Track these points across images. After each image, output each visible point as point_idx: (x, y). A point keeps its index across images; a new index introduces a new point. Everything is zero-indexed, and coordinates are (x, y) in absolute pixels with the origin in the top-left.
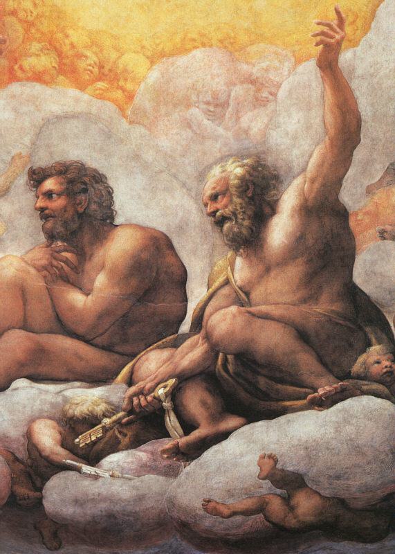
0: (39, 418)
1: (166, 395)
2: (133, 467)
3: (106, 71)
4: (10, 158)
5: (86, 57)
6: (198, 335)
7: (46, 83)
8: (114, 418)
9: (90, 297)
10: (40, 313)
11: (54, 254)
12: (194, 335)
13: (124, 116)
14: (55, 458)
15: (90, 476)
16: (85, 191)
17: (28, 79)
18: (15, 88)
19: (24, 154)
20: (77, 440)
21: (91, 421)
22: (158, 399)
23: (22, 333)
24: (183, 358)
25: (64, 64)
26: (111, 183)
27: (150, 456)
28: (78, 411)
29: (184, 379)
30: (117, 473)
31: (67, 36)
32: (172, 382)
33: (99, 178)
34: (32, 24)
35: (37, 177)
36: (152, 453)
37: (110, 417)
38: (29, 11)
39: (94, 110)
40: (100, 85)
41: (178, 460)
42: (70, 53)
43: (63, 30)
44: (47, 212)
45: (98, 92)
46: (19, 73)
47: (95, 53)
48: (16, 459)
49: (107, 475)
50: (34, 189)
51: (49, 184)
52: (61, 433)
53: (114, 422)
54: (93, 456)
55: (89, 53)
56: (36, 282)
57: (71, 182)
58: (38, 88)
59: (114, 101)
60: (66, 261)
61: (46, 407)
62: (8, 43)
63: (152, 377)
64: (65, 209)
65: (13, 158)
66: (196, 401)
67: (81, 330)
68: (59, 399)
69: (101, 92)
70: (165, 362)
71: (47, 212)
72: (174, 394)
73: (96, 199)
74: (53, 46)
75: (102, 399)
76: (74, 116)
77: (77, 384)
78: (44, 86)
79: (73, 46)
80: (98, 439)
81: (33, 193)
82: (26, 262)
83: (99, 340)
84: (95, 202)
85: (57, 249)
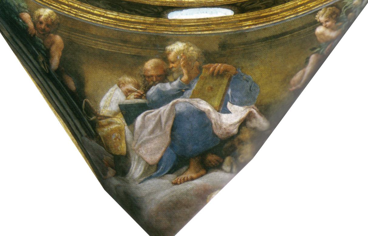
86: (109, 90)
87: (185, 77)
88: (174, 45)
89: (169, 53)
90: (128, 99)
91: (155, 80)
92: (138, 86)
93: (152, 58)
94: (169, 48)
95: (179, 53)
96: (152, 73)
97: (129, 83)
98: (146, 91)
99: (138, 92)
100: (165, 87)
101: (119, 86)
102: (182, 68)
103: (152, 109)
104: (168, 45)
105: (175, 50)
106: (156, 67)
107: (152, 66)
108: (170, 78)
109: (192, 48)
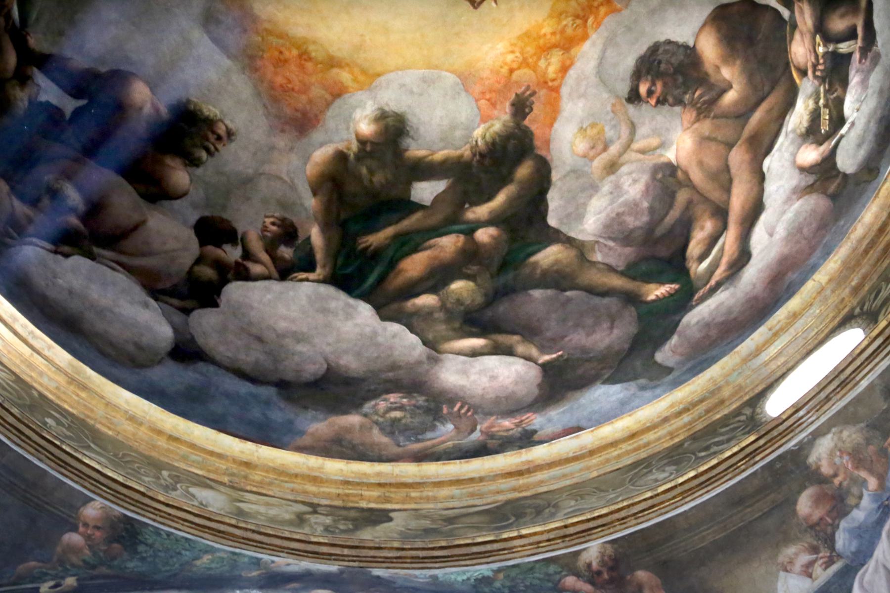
0: (795, 157)
1: (825, 46)
2: (859, 91)
3: (581, 14)
4: (612, 115)
5: (566, 25)
6: (796, 5)
7: (572, 64)
8: (822, 95)
9: (734, 86)
10: (726, 131)
11: (693, 104)
12: (794, 8)
13: (619, 11)
14: (826, 153)
15: (849, 129)
16: (660, 62)
17: (563, 77)
18: (565, 91)
19: (613, 101)
20: (823, 131)
21: (815, 116)
22: (825, 54)
23: (735, 148)
24: (805, 23)
25: (564, 45)
26: (662, 39)
27: (858, 74)
28: (805, 124)
29: (821, 29)
30: (857, 106)
31: (545, 35)
32: (818, 38)
33: (655, 48)
34: (525, 59)
35: (634, 97)
36: (857, 71)
37: (819, 99)
38: (516, 59)
39: (606, 34)
40: (590, 21)
41: (870, 51)
42: (558, 37)
43: (539, 37)
44: (661, 99)
45: (594, 26)
46: (556, 83)
47: (567, 17)
48: (812, 185)
49: (855, 114)
50: (641, 103)
51: (643, 89)
52: (812, 143)
53: (825, 96)
54: (839, 120)
55: (564, 23)
56: (706, 127)
57: (648, 72)
58: (572, 73)
59: (606, 14)
60: (701, 96)
61: (791, 149)
62: (531, 84)
63: (808, 55)
64: (665, 85)
65: (613, 112)
66: (838, 24)
67: (753, 100)
68: (791, 136)
69: (595, 23)
70: (803, 40)
71: (661, 99)
72: (828, 39)
73: (669, 55)
74: (546, 50)
75: (805, 101)
76: (604, 51)
77: (788, 117)
78: (573, 67)
79: (554, 33)
80: (830, 114)
81: (644, 105)
82: (688, 128)
83: (766, 88)
84: (671, 57)
85: (690, 100)
86: (777, 589)
87: (873, 483)
88: (814, 450)
89: (818, 468)
90: (816, 579)
91: (829, 520)
92: (815, 550)
93: (799, 492)
94: (812, 459)
95: (831, 454)
96: (817, 514)
97: (796, 554)
98: (832, 548)
99: (822, 558)
100: (853, 519)
101: (787, 571)
102: (856, 472)
103: (863, 565)
104: (807, 457)
105: (824, 456)
106: (818, 500)
107: (809, 504)
108: (851, 501)
109: (845, 434)
